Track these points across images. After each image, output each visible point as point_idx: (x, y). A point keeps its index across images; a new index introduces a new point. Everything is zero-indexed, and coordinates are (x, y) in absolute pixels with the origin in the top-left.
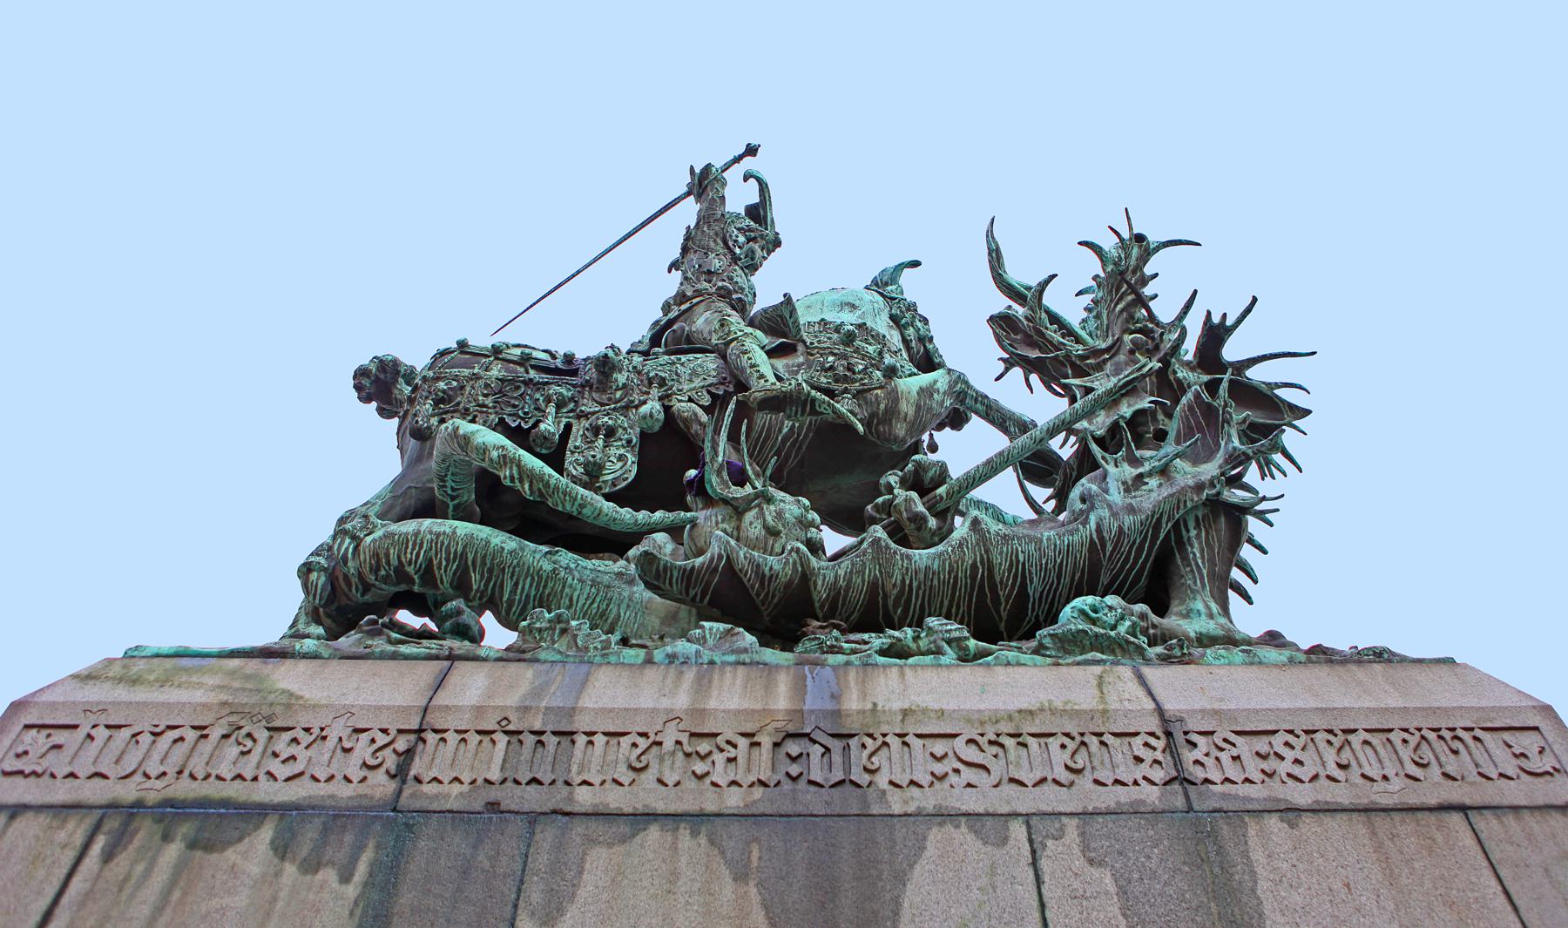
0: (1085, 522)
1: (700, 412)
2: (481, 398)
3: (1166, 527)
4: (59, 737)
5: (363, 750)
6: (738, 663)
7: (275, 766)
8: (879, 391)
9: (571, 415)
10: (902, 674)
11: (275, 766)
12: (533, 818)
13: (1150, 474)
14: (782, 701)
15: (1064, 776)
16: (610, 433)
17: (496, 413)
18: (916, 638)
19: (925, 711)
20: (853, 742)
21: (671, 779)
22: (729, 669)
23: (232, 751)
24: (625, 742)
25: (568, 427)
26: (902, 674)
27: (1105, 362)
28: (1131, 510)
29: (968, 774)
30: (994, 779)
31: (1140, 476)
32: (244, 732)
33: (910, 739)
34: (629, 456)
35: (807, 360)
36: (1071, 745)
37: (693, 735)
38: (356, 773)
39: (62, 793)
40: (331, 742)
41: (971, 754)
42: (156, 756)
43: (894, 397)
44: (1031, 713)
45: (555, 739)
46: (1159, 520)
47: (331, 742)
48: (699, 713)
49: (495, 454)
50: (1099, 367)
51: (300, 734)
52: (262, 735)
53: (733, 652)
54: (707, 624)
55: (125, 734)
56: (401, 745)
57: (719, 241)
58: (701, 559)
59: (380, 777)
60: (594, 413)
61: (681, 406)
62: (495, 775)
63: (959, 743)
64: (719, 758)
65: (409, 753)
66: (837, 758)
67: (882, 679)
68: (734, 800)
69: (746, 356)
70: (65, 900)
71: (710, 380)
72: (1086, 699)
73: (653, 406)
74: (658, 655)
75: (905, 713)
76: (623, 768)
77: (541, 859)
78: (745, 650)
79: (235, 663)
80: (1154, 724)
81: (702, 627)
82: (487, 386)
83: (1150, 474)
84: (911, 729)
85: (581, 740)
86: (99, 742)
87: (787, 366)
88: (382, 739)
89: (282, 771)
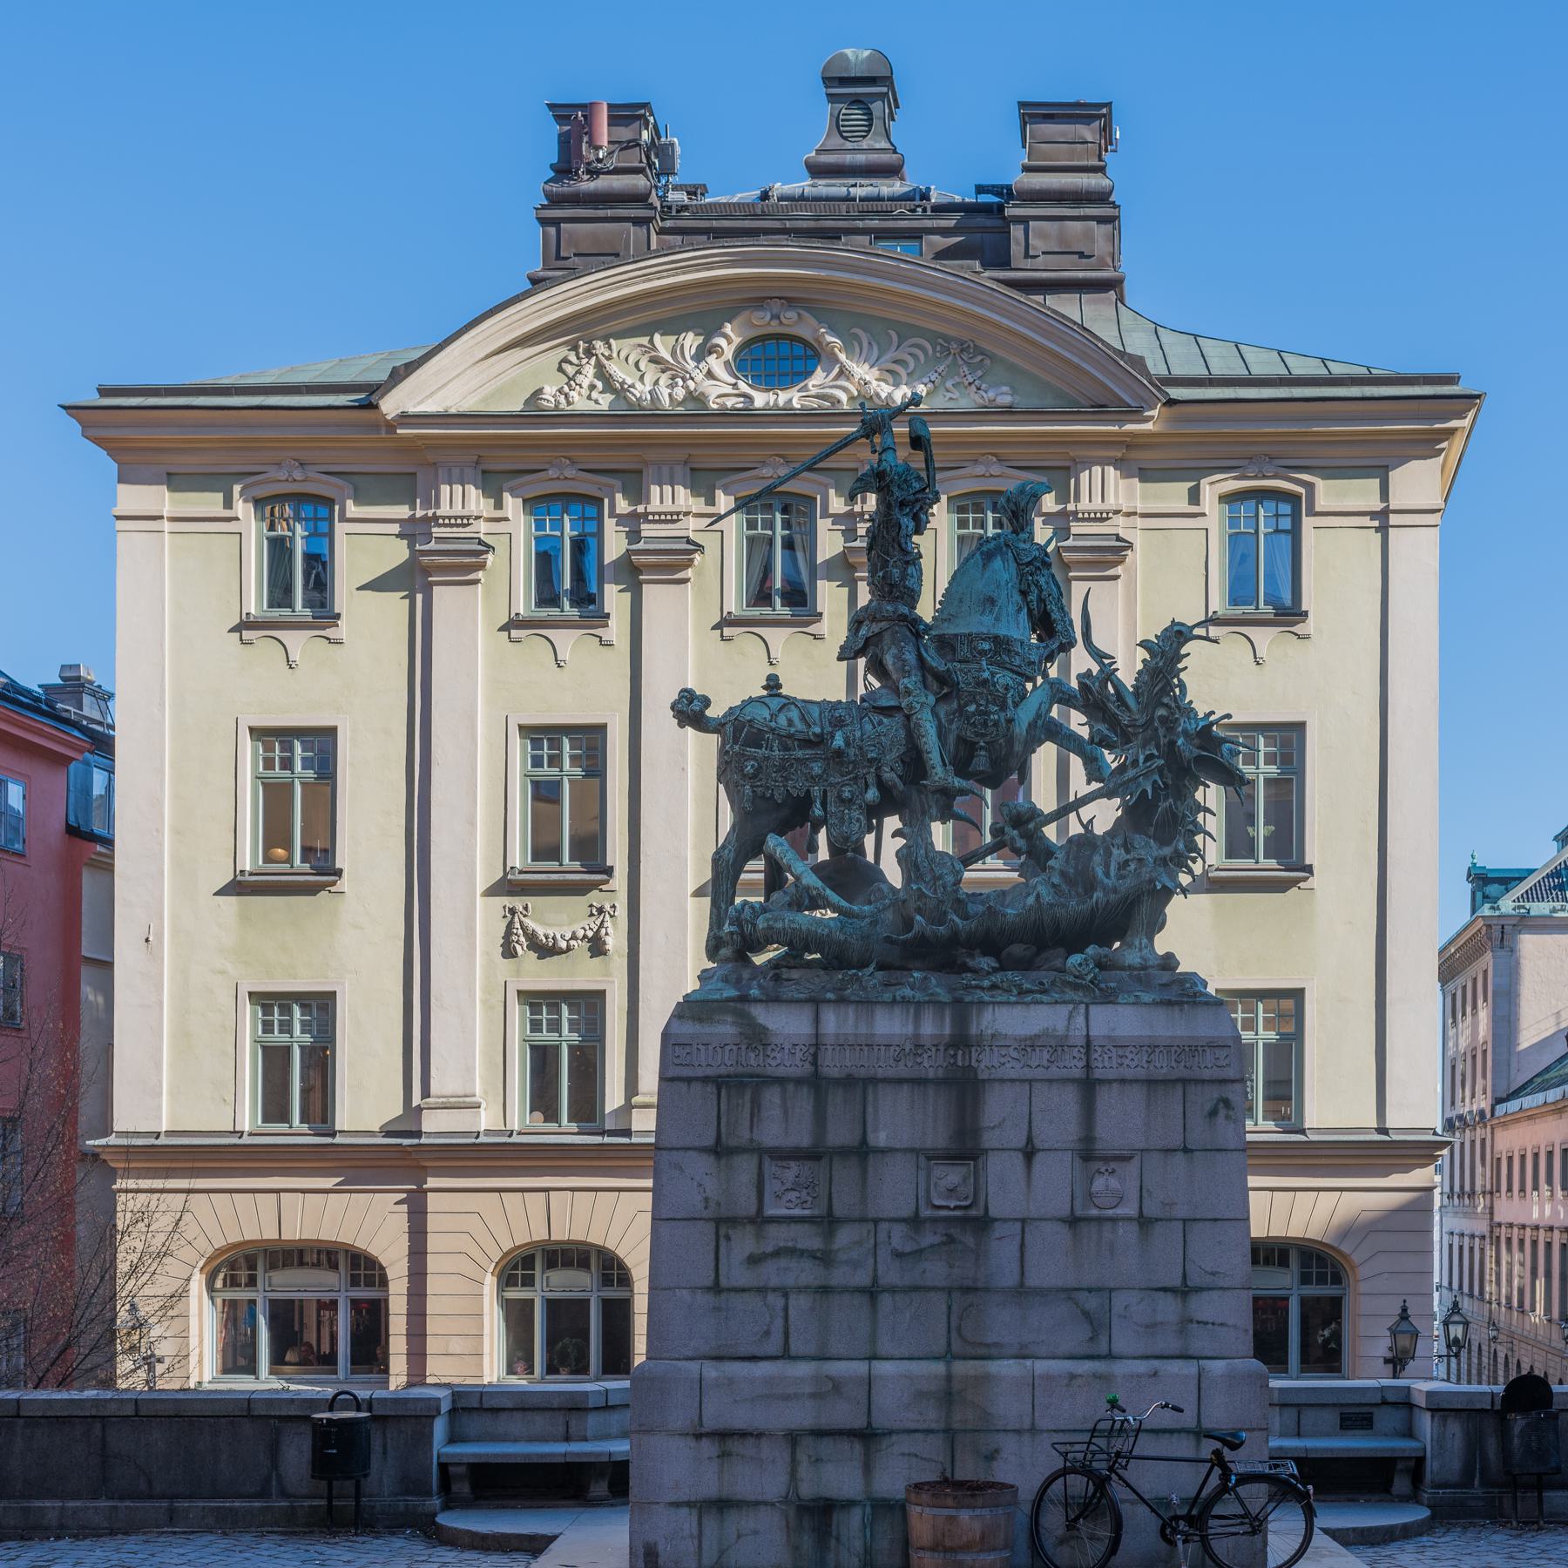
0: (1091, 897)
1: (897, 780)
2: (774, 775)
3: (1131, 898)
4: (688, 1049)
5: (799, 1055)
6: (929, 1002)
7: (769, 1061)
8: (1001, 741)
9: (826, 783)
10: (994, 1010)
11: (769, 1061)
12: (864, 1080)
13: (1132, 860)
14: (947, 1031)
15: (1045, 1063)
16: (848, 802)
17: (784, 786)
18: (1002, 982)
19: (1000, 1034)
20: (973, 1049)
21: (910, 1064)
22: (926, 1006)
23: (753, 1055)
24: (892, 1049)
25: (825, 792)
26: (994, 1010)
27: (1139, 733)
28: (1115, 891)
29: (1013, 1063)
30: (1022, 1065)
31: (1127, 861)
32: (753, 1046)
33: (995, 1049)
34: (861, 817)
35: (959, 705)
36: (1051, 1051)
37: (916, 1046)
38: (800, 1064)
39: (700, 1073)
40: (786, 1051)
41: (1015, 1054)
42: (726, 1058)
43: (1010, 741)
44: (1039, 1036)
45: (866, 1048)
46: (1128, 897)
47: (786, 1051)
48: (917, 1036)
49: (814, 892)
50: (1136, 735)
51: (774, 1047)
52: (761, 1048)
53: (927, 995)
54: (915, 975)
55: (711, 1048)
56: (812, 1050)
57: (896, 546)
58: (910, 935)
59: (807, 1065)
60: (839, 783)
61: (889, 776)
62: (849, 1064)
63: (1011, 1049)
64: (925, 1056)
65: (815, 1056)
66: (967, 1057)
67: (986, 1014)
68: (931, 1074)
69: (924, 739)
70: (722, 1112)
71: (903, 749)
72: (1061, 1027)
73: (872, 794)
74: (898, 998)
75: (993, 1036)
76: (892, 1061)
77: (870, 1098)
78: (932, 994)
79: (731, 1004)
80: (1082, 1042)
81: (913, 977)
82: (775, 766)
83: (1132, 860)
84: (994, 1044)
85: (876, 1048)
86: (703, 1052)
87: (947, 714)
88: (805, 1049)
89: (774, 1063)
